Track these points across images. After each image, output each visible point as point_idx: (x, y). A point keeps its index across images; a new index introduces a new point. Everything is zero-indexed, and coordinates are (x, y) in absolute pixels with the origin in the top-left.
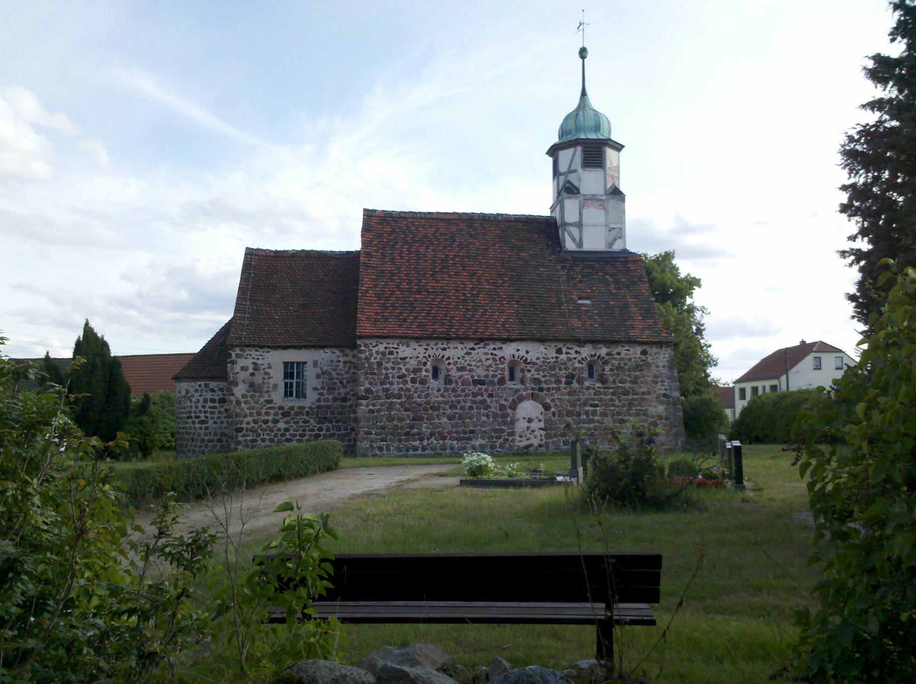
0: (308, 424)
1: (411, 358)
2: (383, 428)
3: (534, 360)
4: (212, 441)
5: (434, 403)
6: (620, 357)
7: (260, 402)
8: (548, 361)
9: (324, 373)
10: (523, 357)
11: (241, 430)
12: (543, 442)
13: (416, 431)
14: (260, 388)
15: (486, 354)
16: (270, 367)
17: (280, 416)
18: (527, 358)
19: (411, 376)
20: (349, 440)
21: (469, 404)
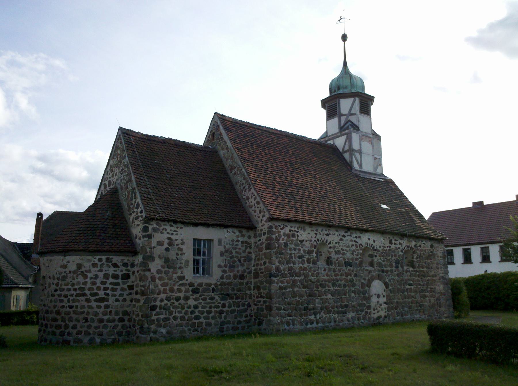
0: (214, 301)
1: (306, 241)
2: (289, 304)
3: (378, 249)
4: (113, 321)
5: (322, 281)
7: (174, 278)
8: (386, 249)
9: (226, 251)
10: (372, 245)
11: (153, 308)
12: (386, 314)
13: (311, 306)
14: (173, 264)
15: (352, 241)
16: (183, 243)
17: (191, 293)
18: (374, 246)
19: (307, 257)
20: (246, 316)
21: (343, 282)
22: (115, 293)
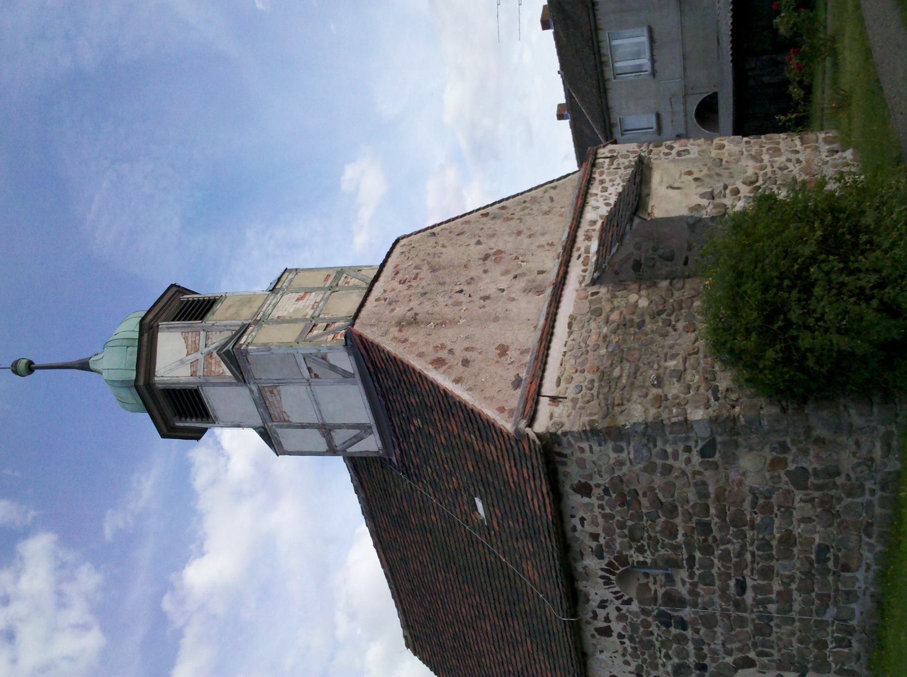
6: (603, 535)
8: (630, 650)
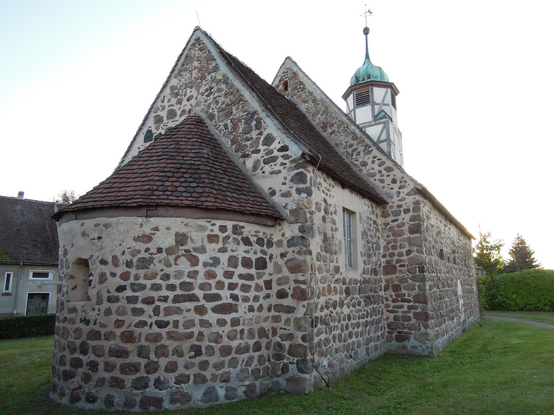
4: (246, 349)
22: (247, 294)
